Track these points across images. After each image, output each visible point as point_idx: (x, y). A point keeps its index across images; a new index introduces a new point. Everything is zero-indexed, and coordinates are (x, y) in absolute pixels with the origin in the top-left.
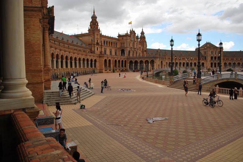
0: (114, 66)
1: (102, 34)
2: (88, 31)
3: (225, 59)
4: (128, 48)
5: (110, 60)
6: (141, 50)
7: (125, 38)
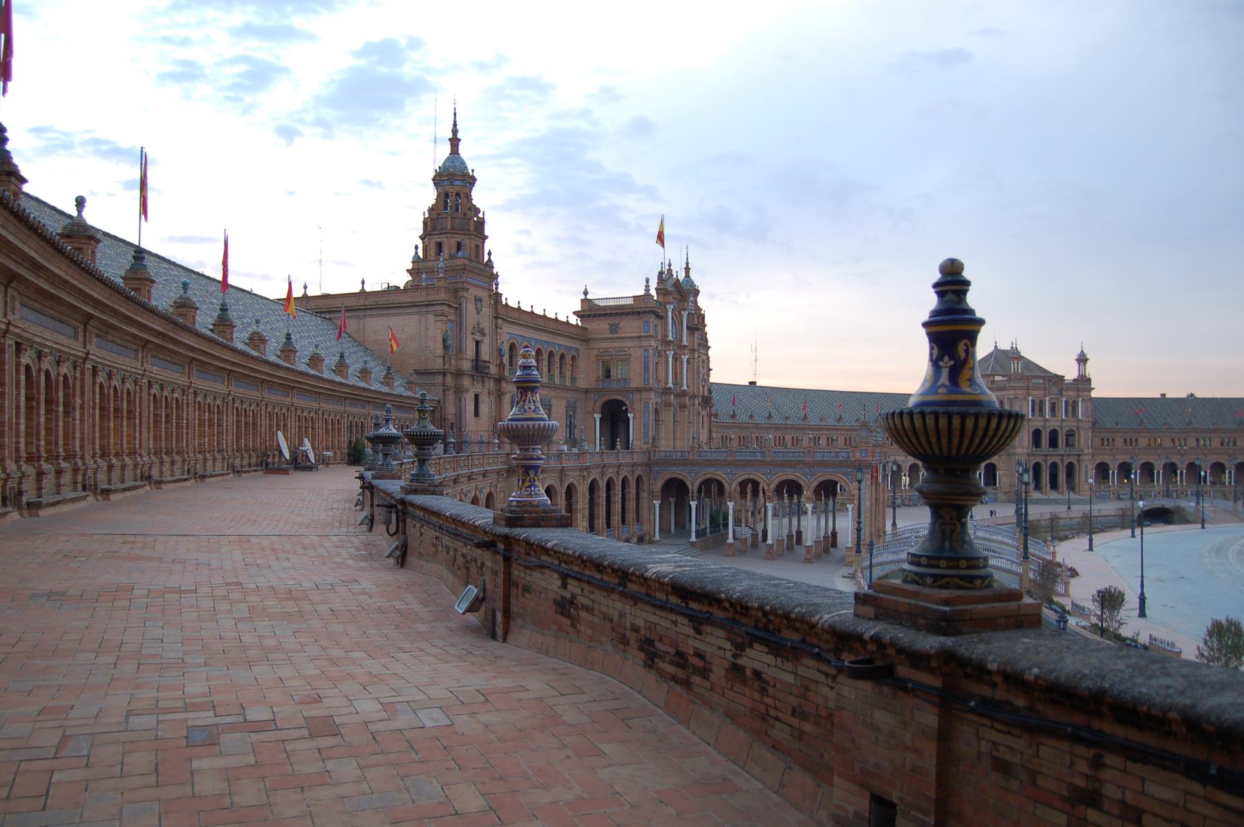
4: (652, 395)
7: (630, 327)
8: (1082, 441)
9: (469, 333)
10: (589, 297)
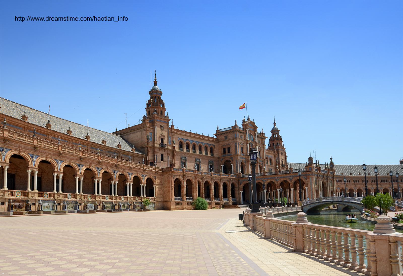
1: (176, 128)
7: (230, 136)
10: (219, 129)
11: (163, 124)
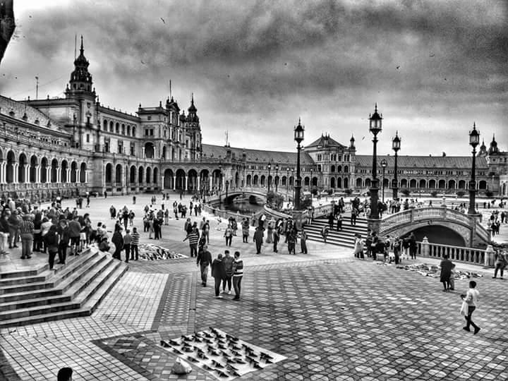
0: (129, 179)
1: (101, 105)
2: (66, 94)
3: (359, 171)
5: (119, 167)
6: (189, 147)
7: (154, 118)
8: (351, 170)
9: (85, 115)
11: (89, 101)
